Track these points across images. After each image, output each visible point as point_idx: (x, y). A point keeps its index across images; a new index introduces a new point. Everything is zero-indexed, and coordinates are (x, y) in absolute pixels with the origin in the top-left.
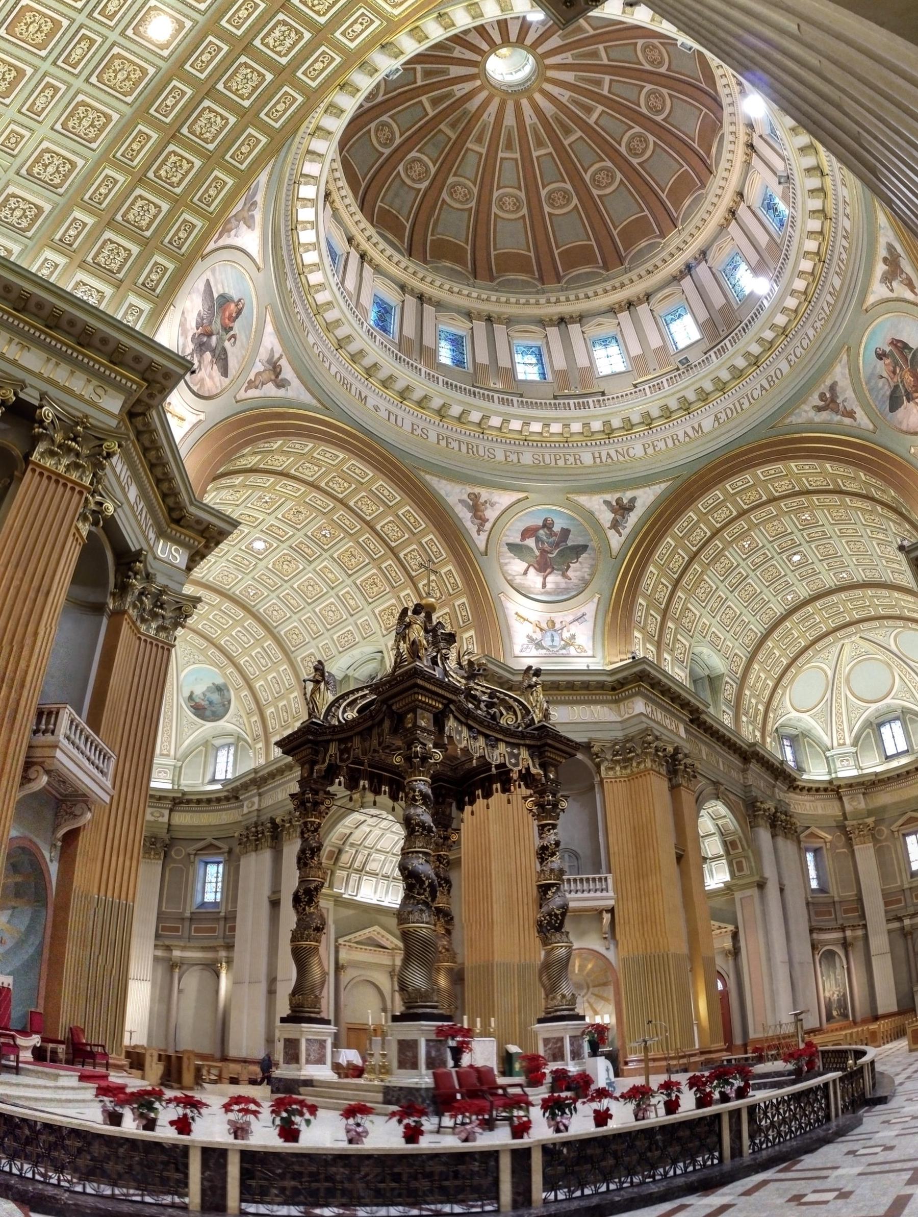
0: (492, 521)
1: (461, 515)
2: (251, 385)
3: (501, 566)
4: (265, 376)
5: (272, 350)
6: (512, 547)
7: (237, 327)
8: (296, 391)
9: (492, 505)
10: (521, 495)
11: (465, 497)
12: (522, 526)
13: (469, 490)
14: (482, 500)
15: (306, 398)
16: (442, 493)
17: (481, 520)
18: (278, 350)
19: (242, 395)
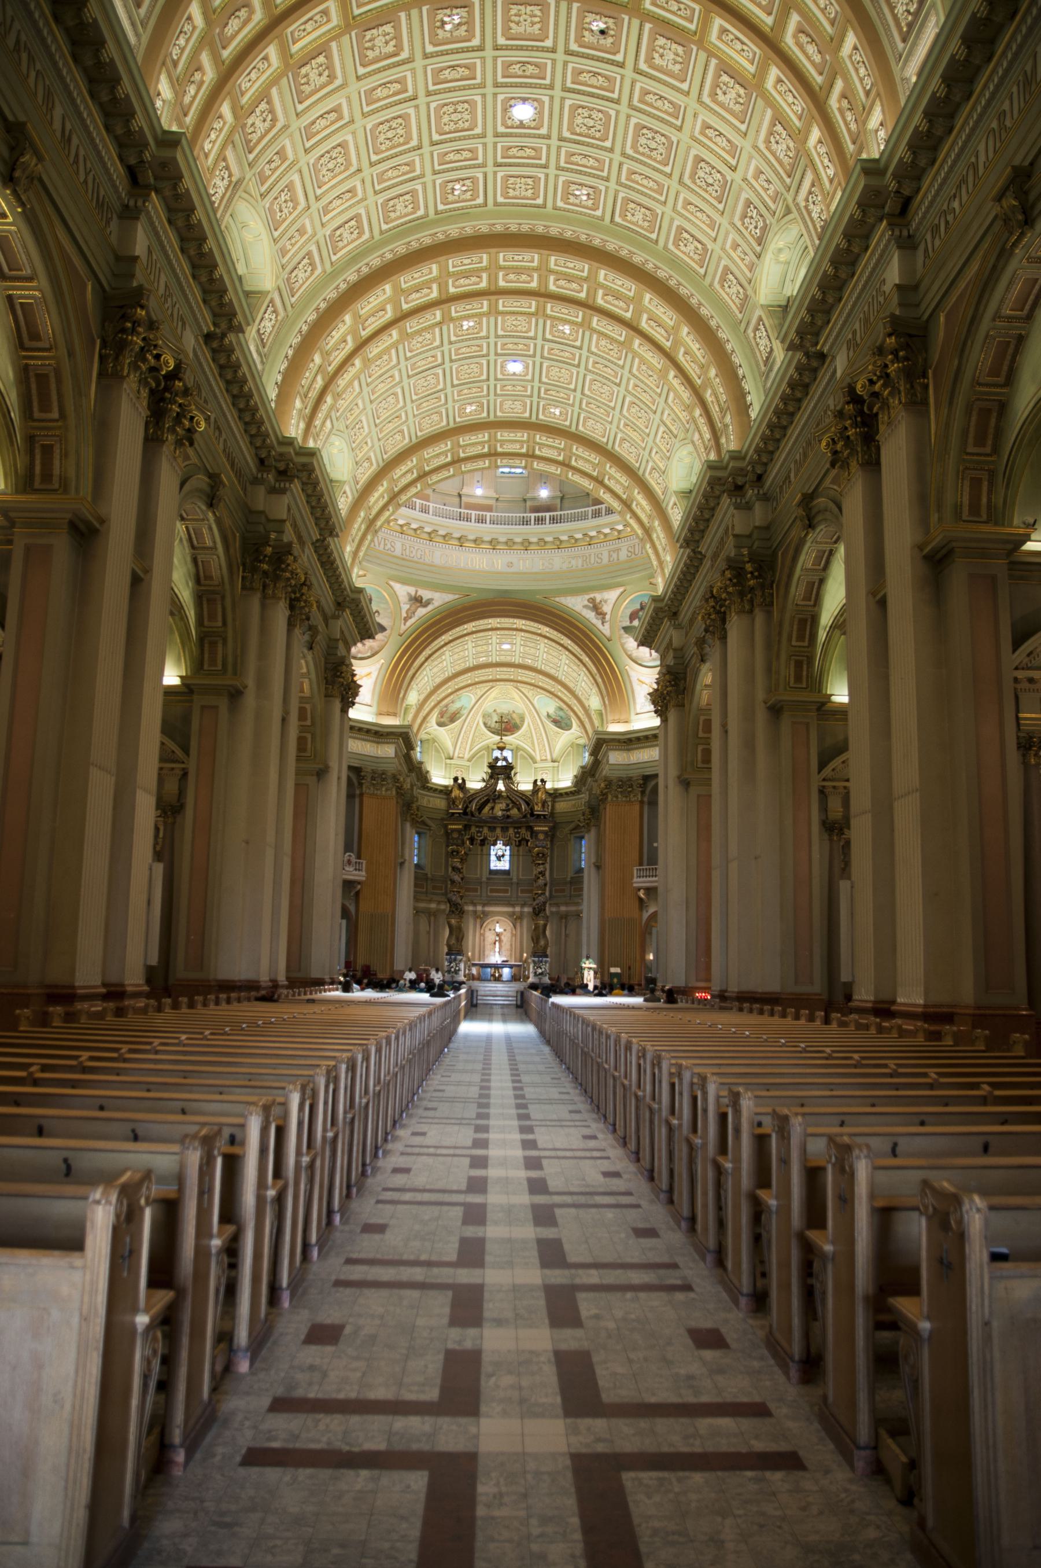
0: (609, 613)
1: (587, 616)
2: (406, 619)
3: (622, 645)
4: (413, 609)
5: (409, 594)
6: (626, 629)
7: (374, 607)
8: (439, 599)
9: (606, 602)
10: (621, 589)
11: (586, 603)
12: (628, 612)
13: (587, 597)
14: (598, 601)
15: (449, 597)
16: (570, 605)
17: (601, 615)
18: (412, 590)
19: (403, 628)
